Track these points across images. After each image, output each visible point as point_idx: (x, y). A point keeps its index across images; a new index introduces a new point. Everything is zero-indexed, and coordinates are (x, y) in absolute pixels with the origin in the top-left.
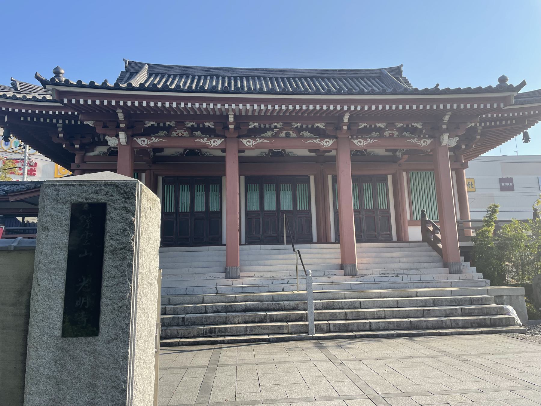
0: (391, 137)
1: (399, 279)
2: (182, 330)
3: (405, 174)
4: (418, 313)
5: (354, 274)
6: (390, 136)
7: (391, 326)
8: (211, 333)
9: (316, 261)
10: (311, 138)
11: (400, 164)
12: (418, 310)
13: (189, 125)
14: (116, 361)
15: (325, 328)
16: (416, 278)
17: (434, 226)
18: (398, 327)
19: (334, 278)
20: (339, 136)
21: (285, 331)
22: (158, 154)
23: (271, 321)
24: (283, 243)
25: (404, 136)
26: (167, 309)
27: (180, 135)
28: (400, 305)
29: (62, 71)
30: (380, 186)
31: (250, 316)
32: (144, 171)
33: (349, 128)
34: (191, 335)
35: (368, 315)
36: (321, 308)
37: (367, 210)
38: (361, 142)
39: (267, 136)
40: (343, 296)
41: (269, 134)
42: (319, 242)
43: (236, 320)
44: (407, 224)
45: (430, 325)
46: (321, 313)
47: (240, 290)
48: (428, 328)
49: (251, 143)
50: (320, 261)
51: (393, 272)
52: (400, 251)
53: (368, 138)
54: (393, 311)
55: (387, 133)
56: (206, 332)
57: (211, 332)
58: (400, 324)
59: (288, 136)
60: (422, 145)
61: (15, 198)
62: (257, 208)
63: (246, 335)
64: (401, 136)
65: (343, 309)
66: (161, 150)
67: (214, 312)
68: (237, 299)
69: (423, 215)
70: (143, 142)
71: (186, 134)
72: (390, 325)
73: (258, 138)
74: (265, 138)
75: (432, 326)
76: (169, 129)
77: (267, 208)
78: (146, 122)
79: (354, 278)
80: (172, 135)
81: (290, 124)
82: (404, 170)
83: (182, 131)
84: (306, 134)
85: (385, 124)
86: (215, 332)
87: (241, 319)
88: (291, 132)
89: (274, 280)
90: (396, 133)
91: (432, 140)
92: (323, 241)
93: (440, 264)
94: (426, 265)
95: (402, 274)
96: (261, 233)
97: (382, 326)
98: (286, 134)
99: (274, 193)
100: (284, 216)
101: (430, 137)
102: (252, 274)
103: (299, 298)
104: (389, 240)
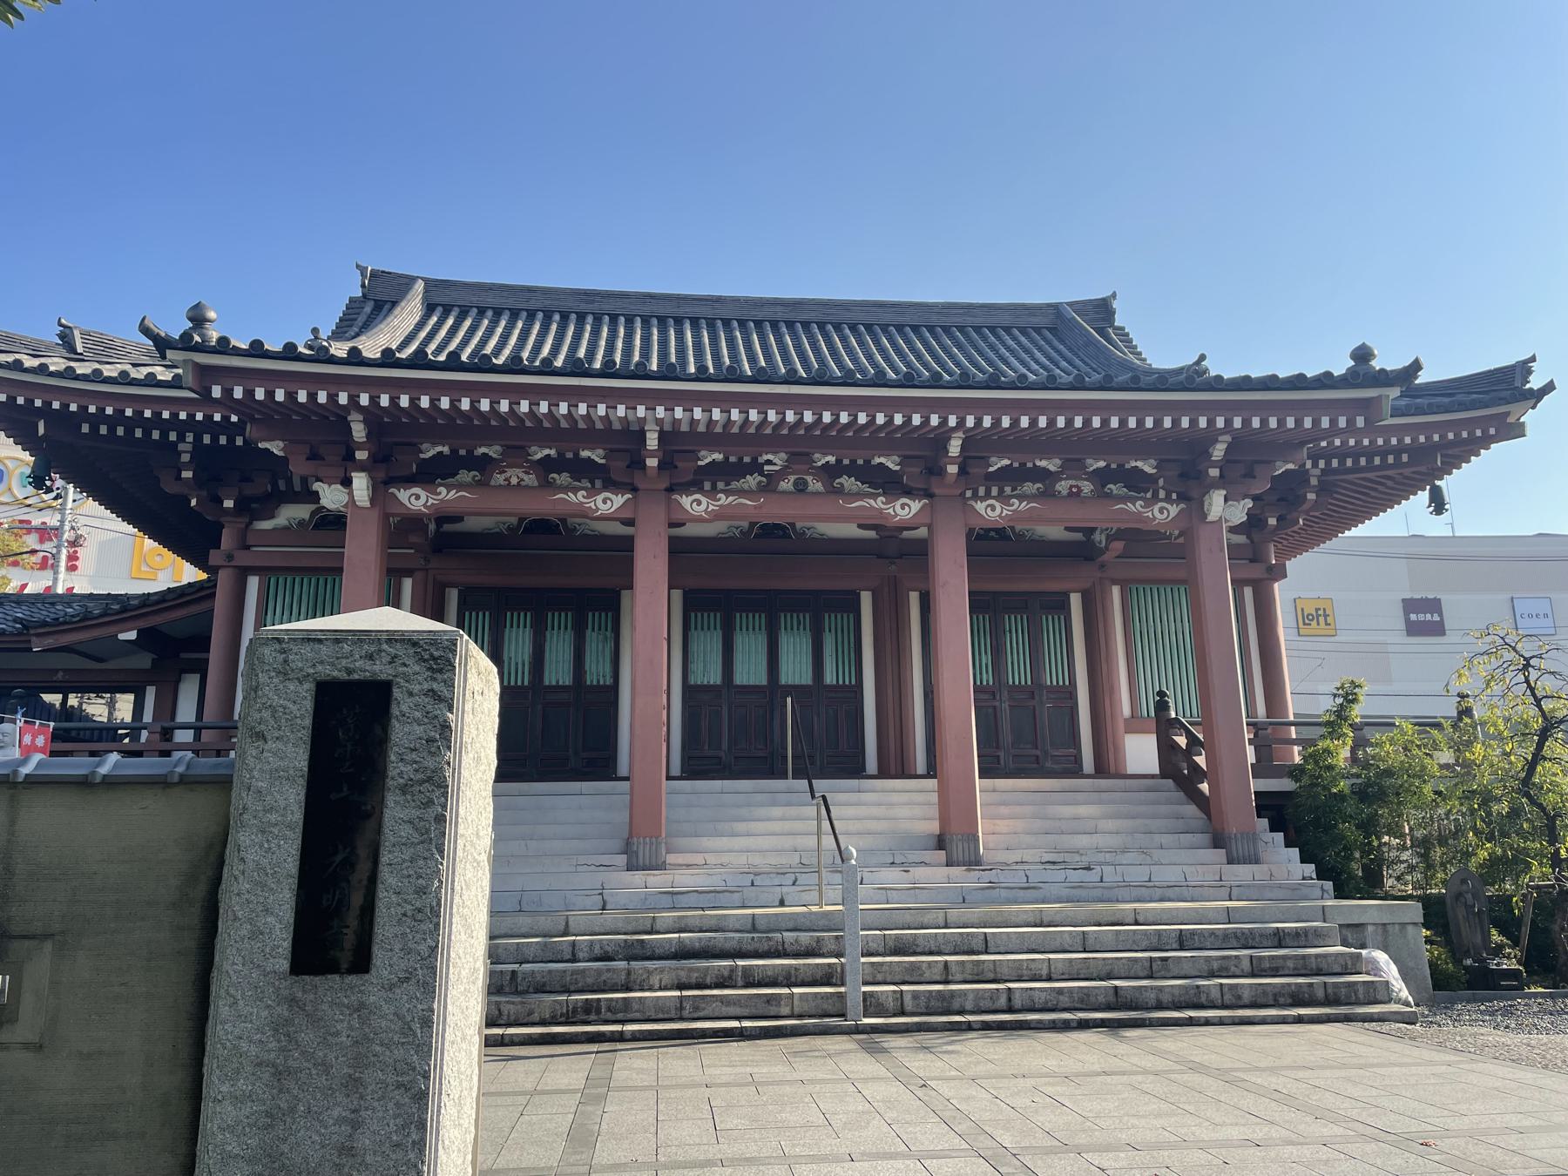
0: (1075, 495)
1: (1093, 876)
3: (1116, 591)
4: (1138, 967)
5: (973, 861)
6: (1071, 494)
7: (1065, 1000)
8: (589, 1012)
11: (1102, 566)
12: (1135, 960)
14: (407, 1030)
15: (891, 1004)
16: (1138, 874)
17: (1189, 735)
18: (1085, 1001)
19: (919, 873)
20: (937, 491)
21: (785, 1011)
22: (447, 527)
23: (747, 985)
25: (1109, 496)
27: (514, 481)
28: (1090, 943)
29: (212, 315)
30: (1049, 623)
31: (691, 970)
32: (409, 573)
33: (963, 471)
34: (536, 1017)
36: (881, 949)
37: (1015, 689)
38: (993, 509)
39: (746, 487)
40: (941, 921)
41: (752, 481)
43: (655, 980)
44: (1121, 726)
45: (1166, 998)
46: (882, 964)
49: (703, 506)
51: (1077, 858)
52: (1100, 802)
54: (1070, 960)
55: (1063, 486)
56: (575, 1010)
59: (801, 487)
61: (50, 642)
62: (714, 677)
63: (682, 1019)
64: (1101, 495)
65: (939, 953)
66: (458, 519)
69: (1162, 706)
70: (415, 499)
71: (530, 479)
73: (722, 491)
77: (740, 678)
78: (424, 446)
80: (493, 483)
81: (806, 457)
82: (1115, 582)
84: (848, 482)
85: (1058, 462)
86: (598, 1012)
87: (666, 979)
88: (809, 478)
89: (756, 874)
91: (1182, 506)
92: (893, 772)
93: (1205, 838)
94: (1166, 839)
95: (1100, 864)
96: (725, 745)
97: (1040, 999)
98: (796, 484)
100: (789, 700)
102: (698, 859)
103: (822, 923)
104: (1073, 770)
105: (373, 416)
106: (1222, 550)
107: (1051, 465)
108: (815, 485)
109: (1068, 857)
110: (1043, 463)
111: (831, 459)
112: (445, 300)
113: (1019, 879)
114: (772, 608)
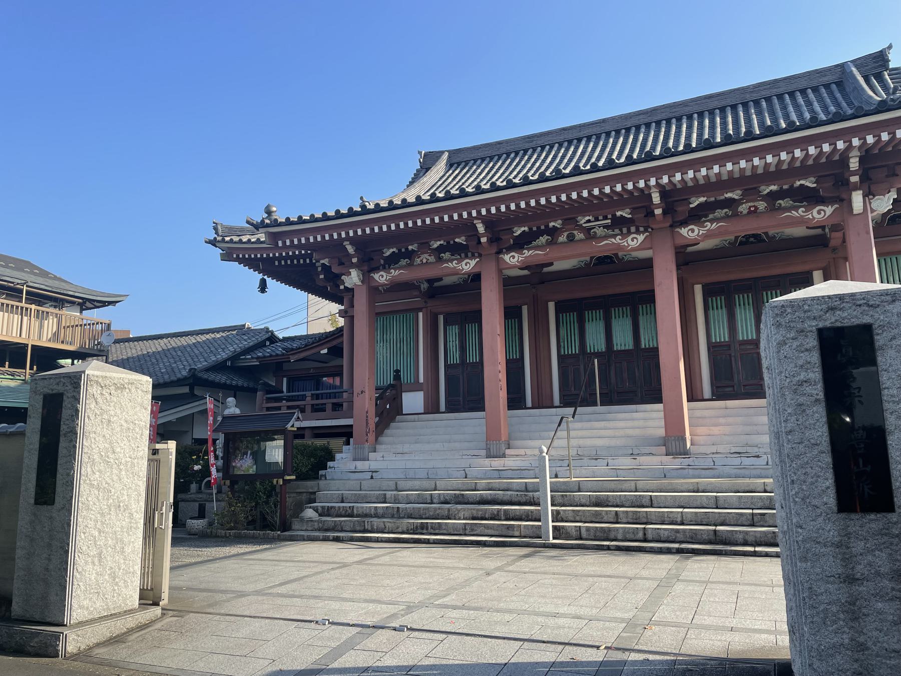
0: (753, 212)
2: (389, 522)
4: (744, 518)
5: (685, 453)
6: (750, 212)
7: (680, 537)
8: (422, 529)
9: (630, 432)
10: (606, 237)
12: (742, 514)
13: (435, 246)
14: (63, 527)
15: (574, 533)
18: (694, 538)
21: (517, 533)
22: (436, 284)
23: (507, 519)
24: (594, 404)
26: (388, 496)
27: (424, 261)
28: (721, 503)
29: (274, 209)
31: (478, 510)
32: (420, 310)
34: (400, 530)
35: (653, 517)
36: (588, 503)
40: (633, 488)
41: (543, 239)
42: (537, 405)
43: (461, 515)
45: (750, 539)
46: (579, 511)
47: (496, 474)
48: (746, 544)
49: (516, 259)
50: (637, 432)
53: (706, 221)
54: (696, 513)
55: (743, 208)
56: (417, 527)
57: (422, 528)
58: (696, 534)
59: (571, 238)
60: (814, 218)
61: (297, 357)
62: (575, 349)
63: (466, 535)
65: (622, 506)
66: (441, 279)
67: (442, 503)
68: (478, 487)
70: (381, 278)
71: (432, 259)
72: (678, 535)
73: (526, 249)
74: (537, 248)
75: (756, 541)
76: (410, 255)
78: (385, 250)
79: (677, 460)
83: (426, 256)
86: (427, 529)
87: (467, 515)
88: (575, 232)
90: (762, 205)
91: (837, 206)
97: (665, 535)
98: (568, 237)
99: (601, 326)
100: (596, 361)
102: (522, 452)
103: (563, 487)
105: (353, 241)
106: (868, 233)
107: (735, 195)
108: (579, 236)
109: (749, 449)
110: (729, 195)
111: (774, 188)
112: (460, 160)
113: (708, 463)
114: (606, 306)
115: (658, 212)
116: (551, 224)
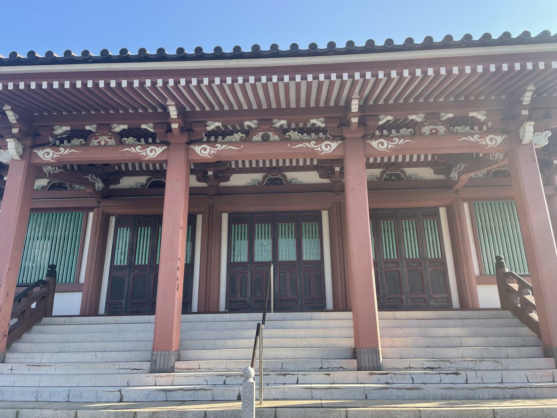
0: (434, 134)
1: (460, 379)
3: (466, 206)
5: (376, 367)
6: (431, 134)
10: (301, 141)
11: (457, 191)
16: (493, 378)
17: (520, 282)
19: (336, 375)
20: (347, 135)
25: (457, 133)
27: (103, 143)
30: (428, 224)
32: (91, 209)
33: (362, 123)
37: (409, 261)
38: (382, 144)
39: (234, 140)
41: (237, 136)
44: (474, 281)
47: (162, 397)
51: (448, 365)
52: (464, 326)
55: (426, 130)
59: (266, 138)
60: (487, 145)
64: (449, 133)
69: (499, 265)
70: (46, 155)
71: (112, 142)
74: (230, 143)
77: (258, 258)
80: (91, 144)
81: (269, 122)
82: (465, 200)
83: (106, 138)
84: (294, 135)
85: (422, 115)
88: (271, 134)
89: (228, 376)
90: (442, 129)
91: (505, 136)
92: (341, 308)
93: (537, 350)
94: (511, 351)
95: (465, 370)
96: (249, 295)
98: (263, 137)
101: (502, 132)
104: (447, 306)
106: (534, 161)
107: (417, 118)
108: (274, 137)
109: (442, 365)
110: (413, 117)
113: (406, 382)
114: (274, 221)
115: (355, 120)
116: (247, 123)
